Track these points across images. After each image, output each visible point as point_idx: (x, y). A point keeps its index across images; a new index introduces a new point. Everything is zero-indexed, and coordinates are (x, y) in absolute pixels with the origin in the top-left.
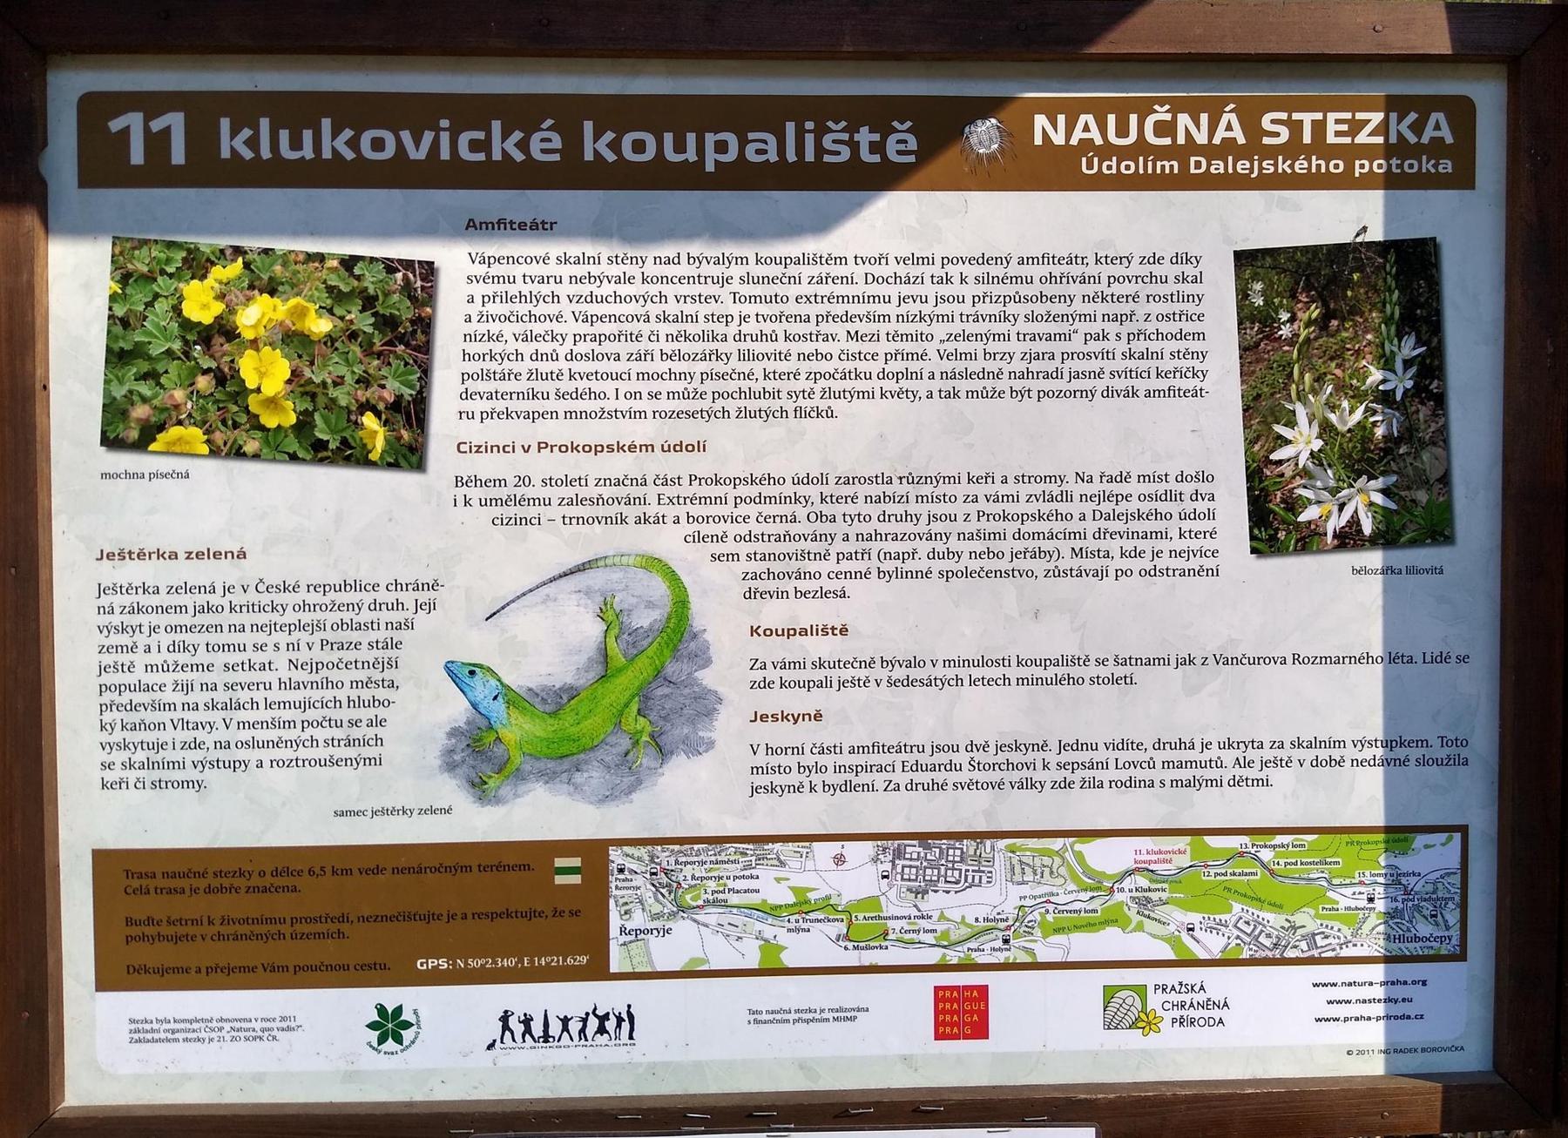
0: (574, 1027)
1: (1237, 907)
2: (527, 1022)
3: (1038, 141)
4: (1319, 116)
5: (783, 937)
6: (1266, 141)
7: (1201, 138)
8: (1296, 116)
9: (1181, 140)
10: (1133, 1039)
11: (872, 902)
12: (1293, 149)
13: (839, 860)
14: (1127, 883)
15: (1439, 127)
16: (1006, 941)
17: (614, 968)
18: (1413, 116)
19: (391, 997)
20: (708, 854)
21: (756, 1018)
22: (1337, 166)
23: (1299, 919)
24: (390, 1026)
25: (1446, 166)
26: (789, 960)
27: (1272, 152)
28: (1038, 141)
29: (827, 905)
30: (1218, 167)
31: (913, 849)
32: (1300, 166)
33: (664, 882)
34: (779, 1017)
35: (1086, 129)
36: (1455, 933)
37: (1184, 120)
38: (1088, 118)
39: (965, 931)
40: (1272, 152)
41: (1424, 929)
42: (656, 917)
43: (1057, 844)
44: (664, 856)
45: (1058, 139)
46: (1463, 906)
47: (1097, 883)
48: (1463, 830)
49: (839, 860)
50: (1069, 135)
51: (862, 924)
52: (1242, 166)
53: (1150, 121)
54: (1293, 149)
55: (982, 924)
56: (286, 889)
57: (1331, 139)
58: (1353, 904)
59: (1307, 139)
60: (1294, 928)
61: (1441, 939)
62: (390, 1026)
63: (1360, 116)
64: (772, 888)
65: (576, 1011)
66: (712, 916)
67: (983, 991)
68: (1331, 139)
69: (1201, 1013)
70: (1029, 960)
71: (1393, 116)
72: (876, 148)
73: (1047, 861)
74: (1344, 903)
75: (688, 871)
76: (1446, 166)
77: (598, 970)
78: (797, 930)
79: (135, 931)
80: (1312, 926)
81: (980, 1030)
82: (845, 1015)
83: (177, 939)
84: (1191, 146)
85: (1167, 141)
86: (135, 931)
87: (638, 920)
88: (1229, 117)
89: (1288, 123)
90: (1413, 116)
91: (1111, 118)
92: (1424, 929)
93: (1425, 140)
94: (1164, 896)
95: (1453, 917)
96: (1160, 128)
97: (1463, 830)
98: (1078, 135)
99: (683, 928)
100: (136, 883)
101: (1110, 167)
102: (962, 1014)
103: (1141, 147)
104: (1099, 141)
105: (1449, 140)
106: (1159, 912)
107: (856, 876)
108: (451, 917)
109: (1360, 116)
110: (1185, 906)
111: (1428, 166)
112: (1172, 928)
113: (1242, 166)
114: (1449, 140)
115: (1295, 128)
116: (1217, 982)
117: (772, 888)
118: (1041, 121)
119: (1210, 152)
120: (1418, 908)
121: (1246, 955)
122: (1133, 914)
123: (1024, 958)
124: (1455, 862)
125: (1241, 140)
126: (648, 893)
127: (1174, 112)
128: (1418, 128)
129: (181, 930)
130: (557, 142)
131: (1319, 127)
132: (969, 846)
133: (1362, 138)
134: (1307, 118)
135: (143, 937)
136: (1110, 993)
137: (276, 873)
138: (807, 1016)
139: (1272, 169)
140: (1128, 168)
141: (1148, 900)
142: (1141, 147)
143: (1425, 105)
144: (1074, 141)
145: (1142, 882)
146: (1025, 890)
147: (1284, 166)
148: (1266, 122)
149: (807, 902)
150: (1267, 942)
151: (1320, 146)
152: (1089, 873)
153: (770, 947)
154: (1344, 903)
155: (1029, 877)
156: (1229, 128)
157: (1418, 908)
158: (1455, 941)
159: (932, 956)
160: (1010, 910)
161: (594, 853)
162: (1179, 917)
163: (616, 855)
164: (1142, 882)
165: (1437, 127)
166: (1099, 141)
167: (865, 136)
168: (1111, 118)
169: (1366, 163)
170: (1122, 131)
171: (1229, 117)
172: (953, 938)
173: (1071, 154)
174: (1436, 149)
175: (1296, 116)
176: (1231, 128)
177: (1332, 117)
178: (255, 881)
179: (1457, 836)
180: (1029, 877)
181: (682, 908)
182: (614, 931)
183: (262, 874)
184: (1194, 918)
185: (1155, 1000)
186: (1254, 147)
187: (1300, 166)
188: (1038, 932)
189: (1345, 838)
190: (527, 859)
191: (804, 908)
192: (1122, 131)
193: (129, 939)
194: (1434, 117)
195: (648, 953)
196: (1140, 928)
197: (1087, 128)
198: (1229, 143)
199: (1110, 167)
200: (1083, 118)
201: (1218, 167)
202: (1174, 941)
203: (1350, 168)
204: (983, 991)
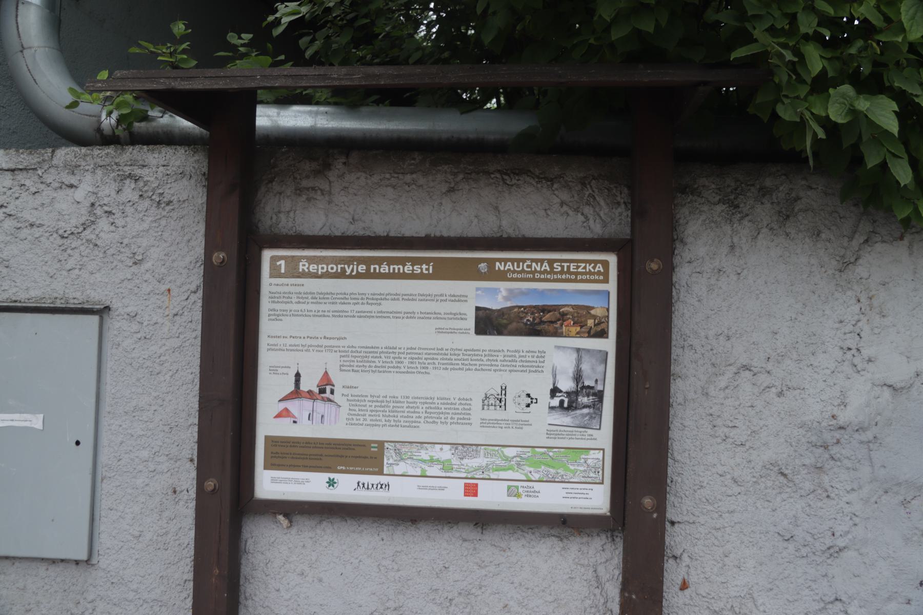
5: (427, 468)
7: (538, 269)
10: (514, 500)
11: (449, 460)
12: (562, 272)
13: (441, 449)
15: (600, 268)
19: (332, 476)
20: (409, 446)
21: (419, 487)
22: (573, 277)
23: (559, 471)
24: (331, 483)
25: (601, 278)
26: (428, 474)
27: (556, 273)
29: (438, 460)
30: (542, 276)
31: (460, 447)
32: (564, 277)
33: (398, 452)
34: (425, 488)
37: (534, 264)
38: (509, 263)
40: (556, 273)
41: (592, 475)
43: (497, 448)
44: (398, 445)
45: (502, 268)
46: (603, 470)
47: (507, 459)
48: (603, 450)
49: (441, 449)
51: (446, 466)
52: (549, 276)
54: (562, 272)
64: (424, 455)
65: (375, 483)
66: (409, 461)
67: (477, 485)
69: (534, 494)
72: (427, 269)
76: (601, 278)
77: (381, 473)
81: (475, 495)
82: (442, 489)
87: (391, 461)
88: (545, 264)
92: (592, 475)
96: (529, 266)
97: (603, 450)
98: (507, 267)
99: (402, 464)
101: (515, 276)
102: (471, 490)
103: (523, 271)
107: (446, 454)
110: (529, 466)
111: (597, 277)
113: (549, 276)
115: (563, 267)
116: (537, 486)
117: (424, 455)
118: (498, 264)
119: (541, 272)
128: (594, 268)
130: (365, 268)
131: (569, 267)
132: (474, 447)
133: (580, 270)
134: (566, 265)
136: (509, 487)
138: (433, 488)
139: (419, 271)
140: (519, 276)
142: (523, 271)
143: (596, 262)
147: (559, 277)
148: (555, 265)
151: (569, 272)
152: (504, 456)
153: (423, 470)
159: (464, 475)
160: (484, 464)
161: (381, 444)
162: (528, 469)
163: (386, 444)
167: (424, 267)
169: (325, 266)
170: (518, 267)
171: (545, 264)
174: (599, 273)
176: (546, 266)
181: (402, 459)
184: (532, 469)
185: (521, 490)
186: (552, 271)
187: (564, 277)
190: (363, 444)
191: (432, 461)
192: (518, 267)
197: (509, 266)
198: (545, 270)
199: (515, 276)
201: (542, 276)
202: (526, 475)
204: (477, 485)
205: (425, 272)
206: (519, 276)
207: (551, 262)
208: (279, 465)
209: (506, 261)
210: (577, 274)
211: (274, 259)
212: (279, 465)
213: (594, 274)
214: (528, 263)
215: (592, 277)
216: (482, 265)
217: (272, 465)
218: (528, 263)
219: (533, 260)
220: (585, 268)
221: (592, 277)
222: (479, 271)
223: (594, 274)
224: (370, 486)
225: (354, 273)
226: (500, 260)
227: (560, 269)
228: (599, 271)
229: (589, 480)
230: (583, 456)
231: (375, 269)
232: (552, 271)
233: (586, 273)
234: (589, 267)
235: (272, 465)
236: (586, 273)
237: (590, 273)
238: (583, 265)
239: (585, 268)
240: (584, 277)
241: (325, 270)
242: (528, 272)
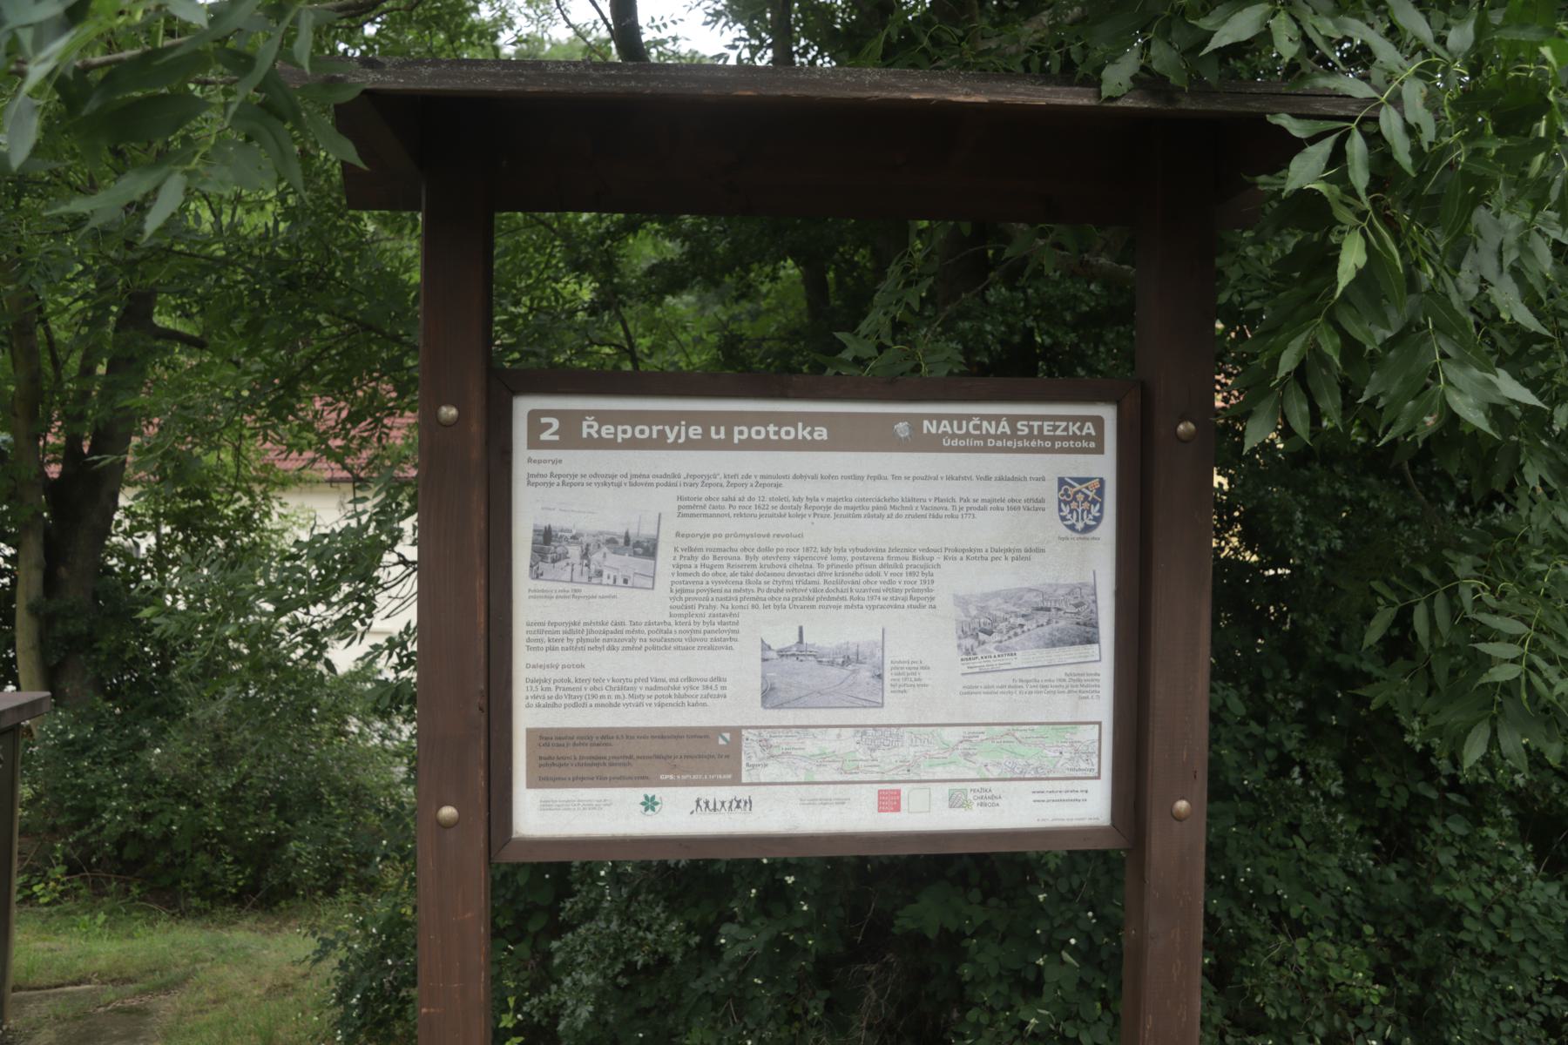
0: (727, 805)
2: (707, 803)
7: (992, 431)
12: (1030, 437)
13: (839, 736)
15: (1089, 429)
19: (650, 791)
22: (1048, 444)
24: (650, 804)
25: (1092, 445)
30: (999, 444)
31: (870, 731)
32: (1033, 444)
33: (765, 745)
37: (985, 424)
38: (945, 422)
40: (1021, 438)
41: (1083, 765)
44: (765, 734)
45: (933, 431)
48: (1100, 724)
52: (1009, 444)
54: (1030, 437)
62: (650, 804)
67: (898, 792)
76: (1092, 445)
77: (736, 781)
81: (897, 808)
84: (988, 435)
87: (754, 761)
88: (1004, 423)
92: (1083, 765)
95: (1095, 760)
96: (977, 427)
97: (1100, 724)
101: (955, 443)
102: (890, 802)
103: (968, 435)
106: (974, 758)
107: (846, 743)
111: (1085, 444)
113: (1009, 444)
115: (1031, 428)
118: (926, 423)
119: (996, 437)
126: (758, 749)
128: (1081, 429)
131: (1041, 428)
132: (894, 730)
133: (1058, 432)
134: (1036, 424)
140: (962, 443)
142: (968, 435)
147: (1026, 444)
148: (1019, 425)
151: (1041, 436)
161: (736, 732)
164: (966, 745)
170: (960, 428)
171: (1004, 423)
174: (1088, 437)
176: (1005, 427)
185: (970, 796)
186: (1014, 435)
187: (1033, 444)
190: (703, 735)
191: (823, 759)
192: (960, 428)
198: (1004, 434)
199: (955, 443)
201: (999, 444)
205: (772, 437)
206: (962, 443)
207: (1013, 420)
209: (939, 418)
210: (1053, 439)
211: (534, 416)
212: (554, 779)
213: (1080, 438)
214: (976, 421)
215: (1078, 444)
216: (901, 424)
217: (541, 779)
218: (976, 421)
219: (983, 417)
220: (1066, 429)
221: (1078, 444)
222: (895, 434)
223: (1080, 438)
224: (719, 806)
225: (681, 440)
226: (931, 417)
227: (1026, 430)
229: (1080, 774)
231: (718, 432)
232: (1014, 435)
233: (1067, 438)
234: (1074, 428)
235: (541, 779)
236: (1067, 438)
237: (1075, 437)
238: (1064, 424)
239: (1066, 429)
240: (1066, 444)
241: (745, 436)
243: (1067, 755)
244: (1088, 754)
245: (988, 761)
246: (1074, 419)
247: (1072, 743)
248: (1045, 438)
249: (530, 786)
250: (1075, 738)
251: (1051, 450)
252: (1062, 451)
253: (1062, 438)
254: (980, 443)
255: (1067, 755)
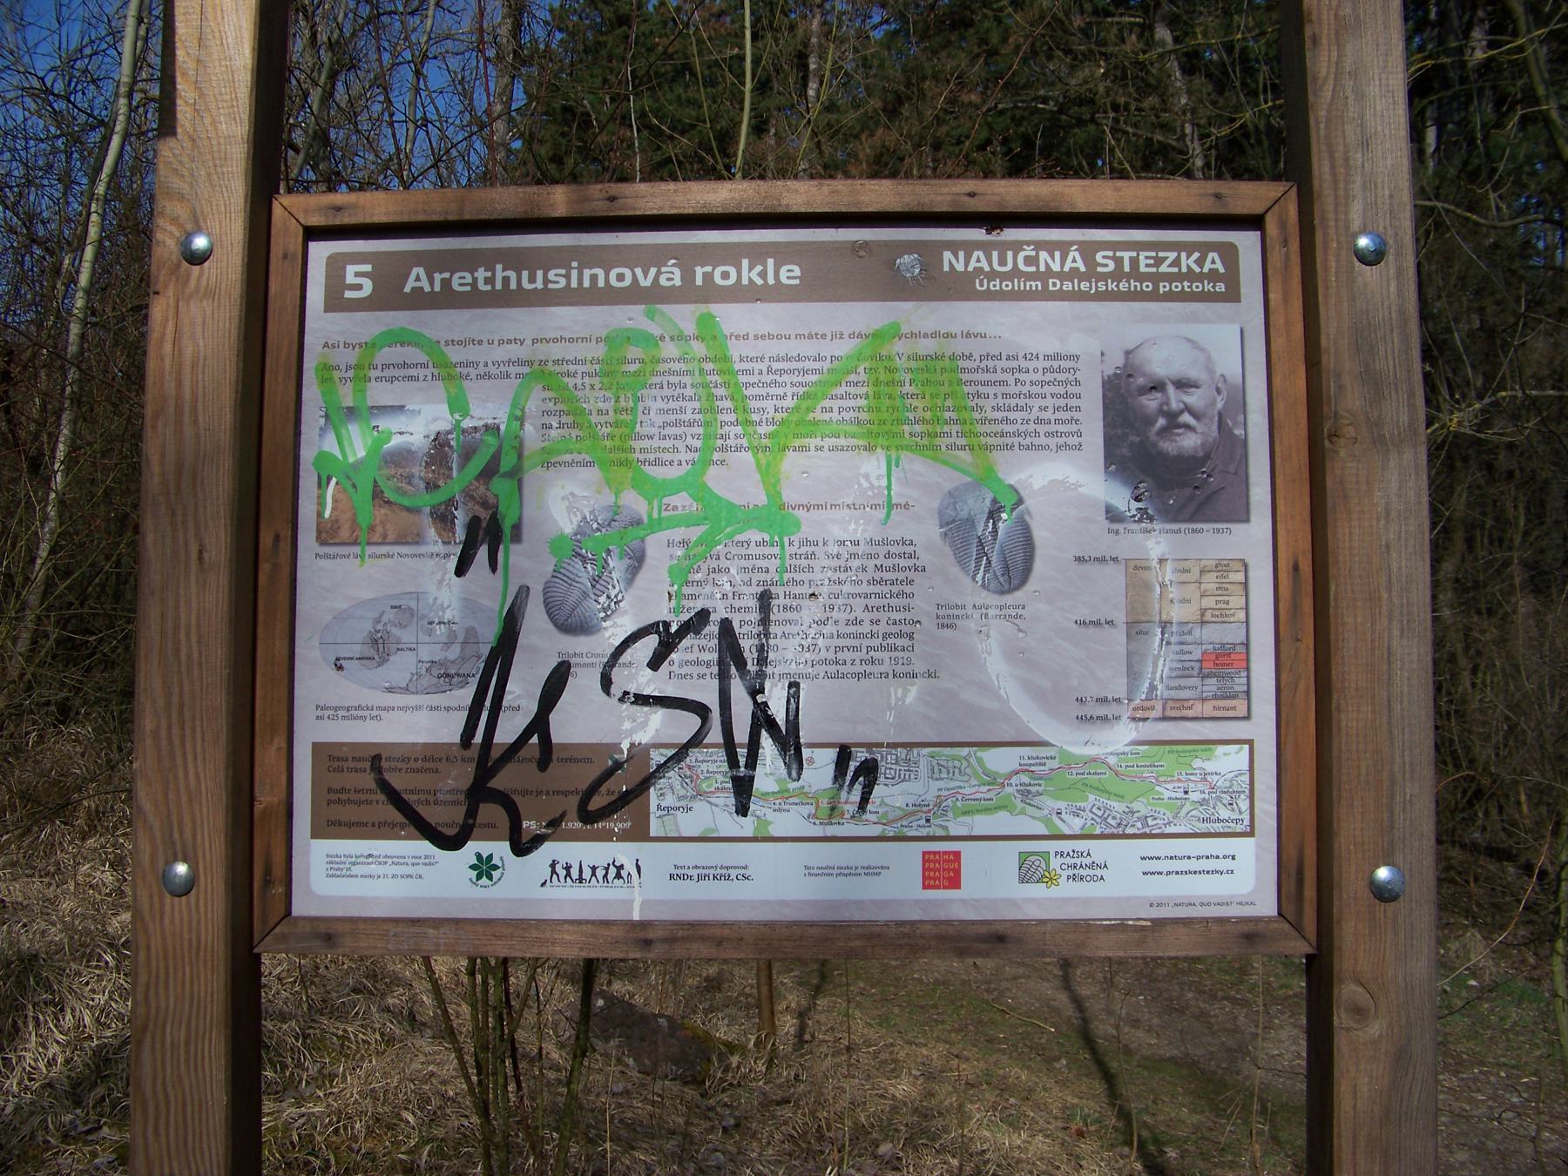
1: (1092, 797)
3: (946, 268)
4: (1134, 254)
5: (770, 815)
6: (1099, 269)
7: (1056, 267)
8: (1118, 254)
9: (1042, 268)
12: (1117, 275)
14: (1014, 780)
15: (1214, 262)
16: (928, 821)
17: (652, 834)
18: (1196, 255)
22: (1148, 287)
23: (1135, 806)
25: (1221, 287)
26: (774, 831)
27: (1104, 277)
28: (946, 268)
30: (1067, 286)
32: (1123, 286)
35: (978, 260)
36: (1246, 817)
37: (1043, 255)
39: (899, 813)
40: (1104, 277)
41: (1224, 813)
42: (680, 798)
43: (964, 751)
45: (960, 267)
47: (992, 779)
48: (1250, 742)
50: (966, 266)
52: (1084, 286)
53: (1021, 255)
54: (1117, 275)
55: (911, 808)
56: (430, 770)
57: (1143, 269)
58: (1174, 795)
59: (1127, 268)
60: (1133, 813)
61: (1237, 821)
63: (1161, 254)
68: (1143, 269)
70: (942, 833)
71: (1183, 255)
73: (957, 763)
74: (1167, 794)
75: (704, 767)
77: (639, 832)
78: (780, 810)
79: (334, 797)
80: (1144, 811)
83: (359, 803)
85: (1033, 269)
86: (334, 797)
87: (670, 800)
88: (1074, 254)
89: (1114, 258)
90: (1196, 255)
91: (995, 254)
93: (1206, 270)
94: (1040, 789)
95: (1244, 805)
96: (1029, 261)
97: (1250, 742)
99: (699, 806)
100: (336, 764)
101: (995, 285)
104: (987, 269)
105: (1222, 270)
108: (539, 793)
109: (1161, 254)
111: (1208, 287)
112: (1046, 812)
113: (1084, 286)
114: (1222, 270)
115: (1119, 262)
118: (947, 255)
119: (1062, 276)
120: (1219, 799)
121: (1098, 831)
122: (1018, 802)
123: (940, 832)
124: (1245, 766)
125: (1083, 269)
127: (1037, 250)
128: (1200, 262)
129: (363, 797)
131: (1134, 262)
134: (1126, 255)
135: (339, 801)
137: (425, 759)
140: (1007, 286)
141: (1029, 792)
144: (970, 269)
145: (1025, 779)
146: (941, 784)
147: (1112, 286)
148: (1099, 257)
149: (787, 790)
150: (1113, 823)
151: (1135, 273)
154: (1167, 794)
155: (944, 775)
156: (1074, 261)
157: (1219, 799)
158: (1247, 822)
159: (876, 830)
160: (930, 797)
162: (1050, 803)
164: (1025, 779)
165: (1213, 262)
166: (987, 269)
168: (995, 254)
170: (1003, 262)
171: (1074, 254)
172: (891, 816)
173: (969, 277)
174: (1213, 276)
175: (1118, 254)
176: (1075, 261)
177: (1142, 255)
178: (412, 765)
179: (1246, 747)
180: (944, 775)
181: (700, 794)
182: (653, 807)
183: (416, 760)
184: (1062, 805)
186: (1091, 273)
188: (950, 814)
189: (1168, 748)
192: (1003, 262)
193: (329, 802)
194: (1211, 255)
195: (676, 823)
196: (1023, 812)
198: (1074, 270)
200: (976, 254)
201: (1067, 286)
202: (1047, 821)
203: (1156, 287)
206: (1007, 286)
208: (350, 825)
210: (1156, 278)
212: (350, 825)
213: (1200, 277)
214: (1029, 251)
215: (1197, 287)
216: (907, 259)
217: (331, 823)
218: (1029, 251)
219: (1039, 245)
220: (1176, 263)
221: (1197, 287)
223: (1200, 277)
226: (954, 247)
227: (1112, 266)
228: (1213, 272)
229: (1218, 827)
230: (1197, 763)
232: (1091, 273)
233: (1179, 277)
234: (1188, 262)
235: (331, 823)
236: (1179, 277)
237: (1191, 276)
238: (1172, 256)
239: (1176, 263)
240: (1176, 287)
242: (1030, 277)
243: (1193, 796)
244: (1234, 794)
245: (1062, 805)
246: (1189, 248)
247: (1205, 776)
248: (1142, 278)
249: (315, 835)
250: (1209, 766)
251: (1154, 296)
252: (1170, 297)
253: (1169, 278)
254: (1036, 285)
255: (1193, 796)
